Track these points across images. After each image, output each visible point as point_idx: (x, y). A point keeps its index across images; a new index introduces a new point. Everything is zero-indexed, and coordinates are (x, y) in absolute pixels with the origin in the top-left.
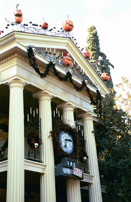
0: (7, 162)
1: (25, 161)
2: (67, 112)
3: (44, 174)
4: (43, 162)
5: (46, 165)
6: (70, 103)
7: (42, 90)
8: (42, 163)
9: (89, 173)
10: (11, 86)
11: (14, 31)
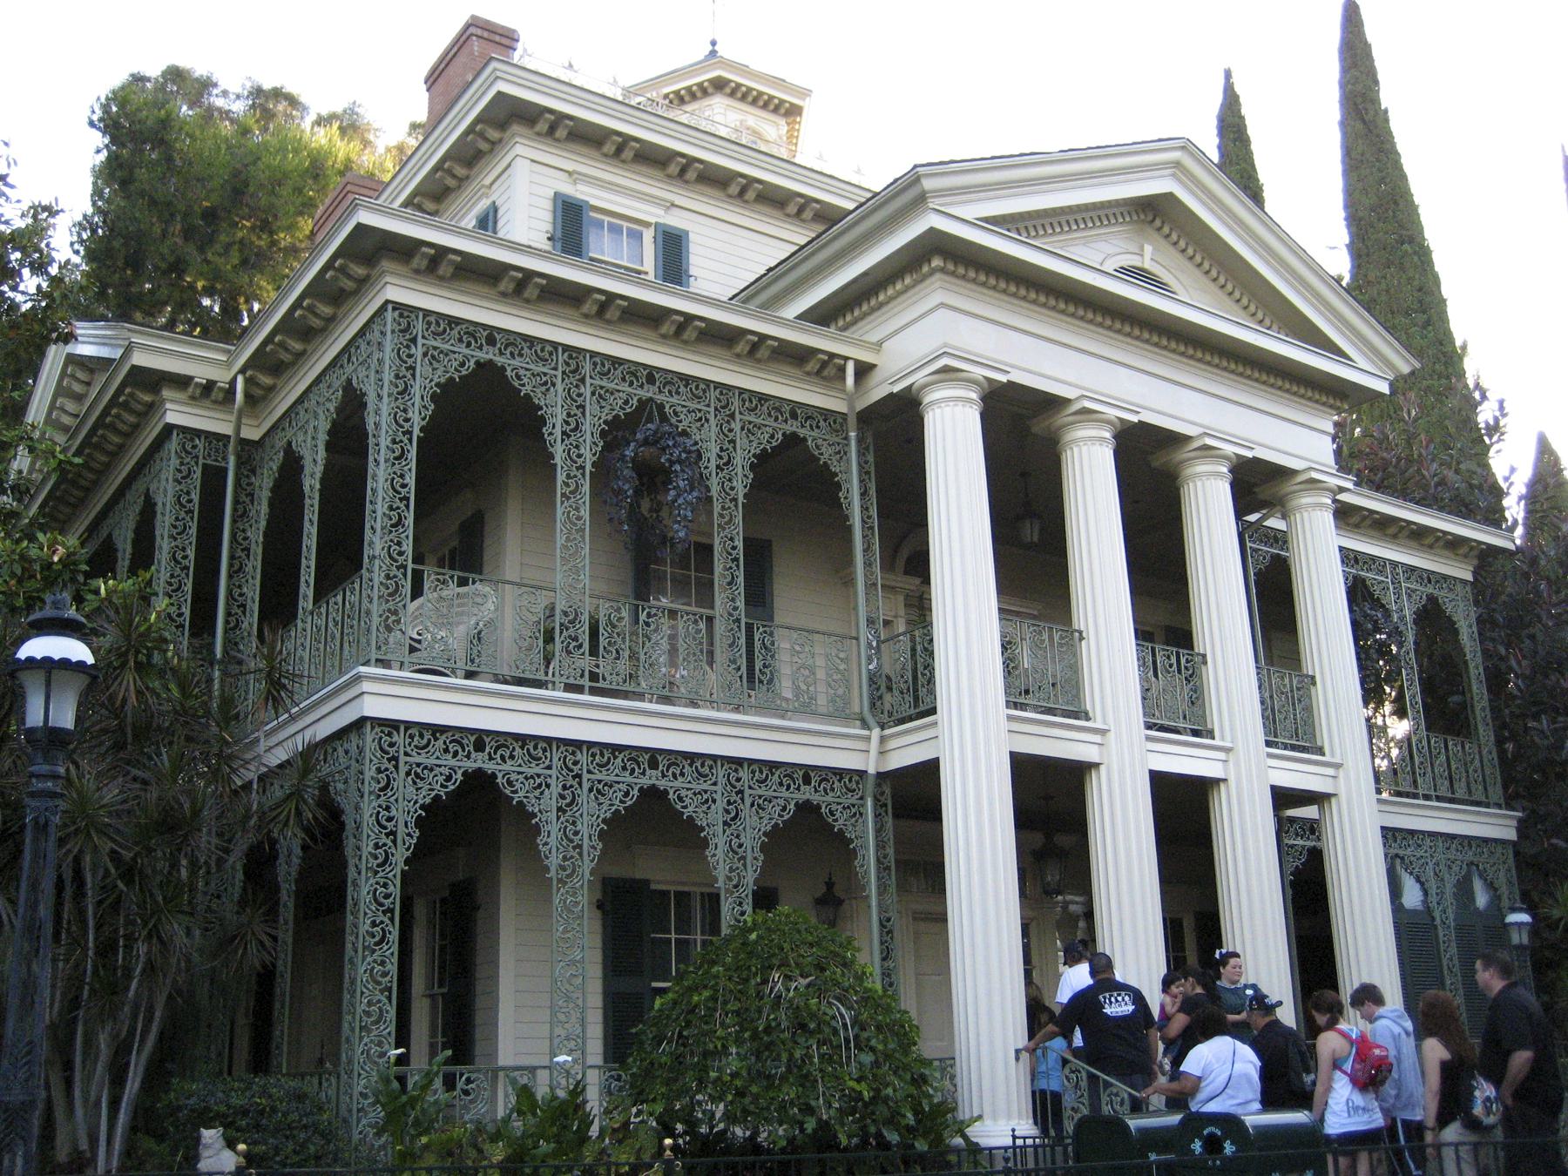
0: (935, 724)
1: (1010, 718)
2: (1199, 484)
3: (1097, 765)
4: (1091, 715)
5: (1106, 727)
6: (1209, 441)
7: (1066, 402)
8: (1088, 719)
9: (1321, 751)
10: (926, 400)
11: (915, 166)
